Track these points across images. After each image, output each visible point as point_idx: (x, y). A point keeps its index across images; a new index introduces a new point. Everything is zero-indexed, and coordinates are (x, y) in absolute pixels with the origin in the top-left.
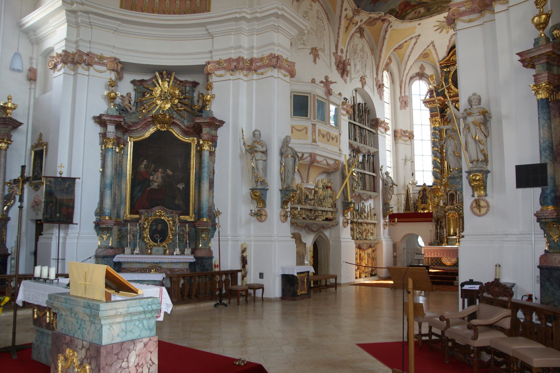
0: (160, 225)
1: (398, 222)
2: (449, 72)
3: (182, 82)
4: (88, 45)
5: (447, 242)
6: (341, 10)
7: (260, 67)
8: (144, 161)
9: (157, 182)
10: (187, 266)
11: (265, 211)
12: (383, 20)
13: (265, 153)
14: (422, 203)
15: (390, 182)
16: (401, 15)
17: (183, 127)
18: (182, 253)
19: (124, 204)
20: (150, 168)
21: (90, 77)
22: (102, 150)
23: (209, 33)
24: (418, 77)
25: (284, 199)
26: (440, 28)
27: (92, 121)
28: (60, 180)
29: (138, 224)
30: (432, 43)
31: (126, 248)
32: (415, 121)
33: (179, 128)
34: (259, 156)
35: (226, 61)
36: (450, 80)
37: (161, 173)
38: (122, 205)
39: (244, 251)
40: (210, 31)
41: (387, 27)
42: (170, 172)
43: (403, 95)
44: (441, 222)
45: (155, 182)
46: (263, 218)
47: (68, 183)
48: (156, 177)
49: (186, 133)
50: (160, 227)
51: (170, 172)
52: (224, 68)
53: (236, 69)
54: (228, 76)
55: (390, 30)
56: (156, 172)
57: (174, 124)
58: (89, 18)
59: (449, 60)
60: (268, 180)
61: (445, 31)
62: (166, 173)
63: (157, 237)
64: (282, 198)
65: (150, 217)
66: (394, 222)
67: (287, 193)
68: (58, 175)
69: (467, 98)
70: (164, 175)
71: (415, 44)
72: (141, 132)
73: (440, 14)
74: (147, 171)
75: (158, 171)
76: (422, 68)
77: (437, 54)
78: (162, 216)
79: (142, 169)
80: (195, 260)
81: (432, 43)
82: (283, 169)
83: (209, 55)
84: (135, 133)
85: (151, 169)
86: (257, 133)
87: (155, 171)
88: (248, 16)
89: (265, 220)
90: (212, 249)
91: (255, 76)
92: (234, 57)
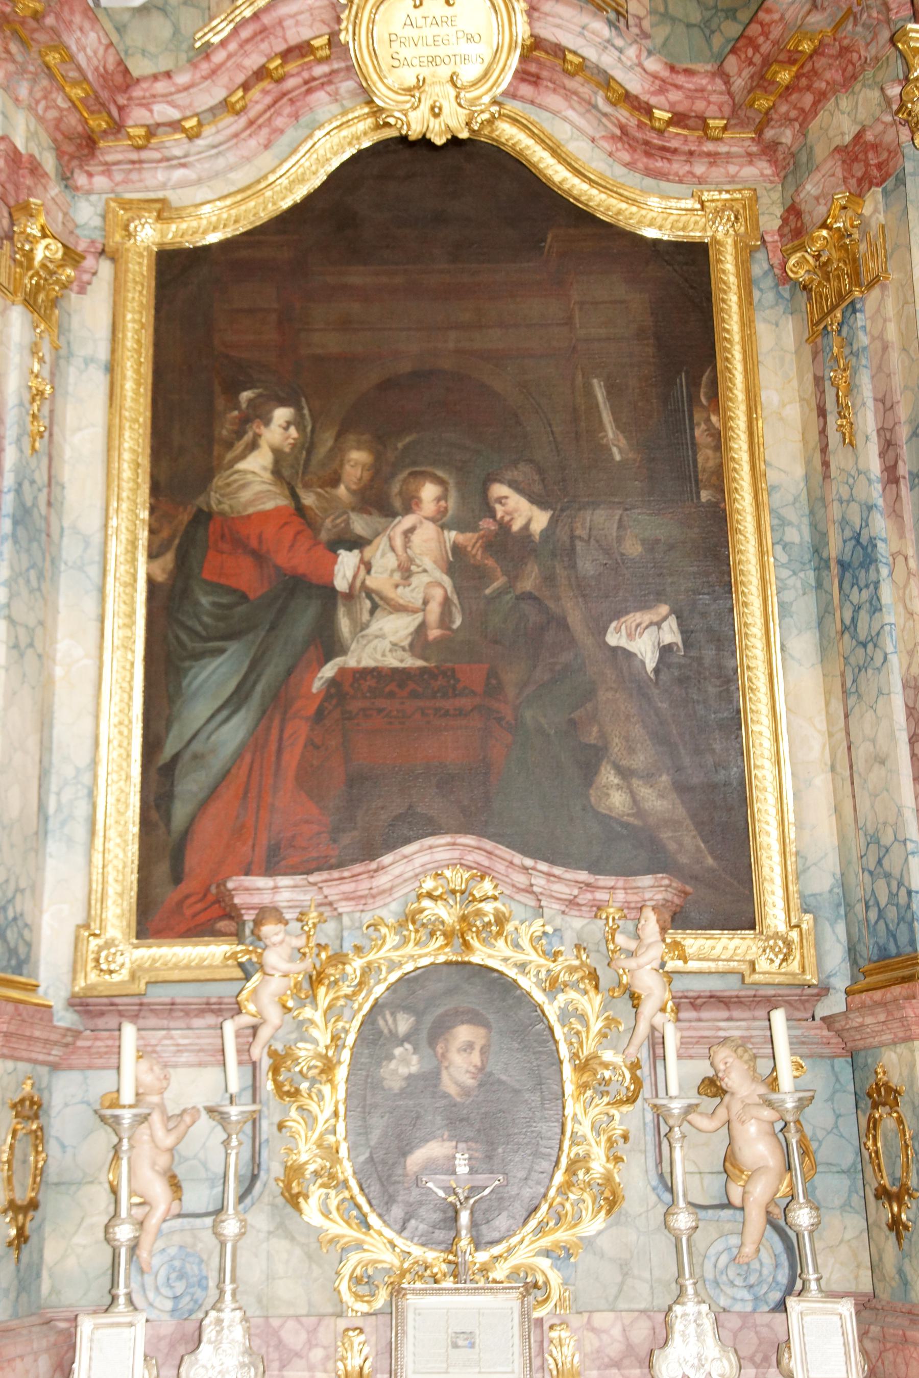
0: (464, 1033)
8: (267, 422)
9: (399, 608)
19: (80, 832)
20: (335, 481)
29: (230, 1027)
31: (86, 1325)
37: (441, 521)
38: (53, 846)
48: (391, 561)
56: (389, 512)
62: (487, 525)
65: (358, 949)
70: (465, 538)
72: (232, 157)
74: (300, 510)
75: (410, 504)
79: (246, 495)
84: (179, 174)
85: (342, 490)
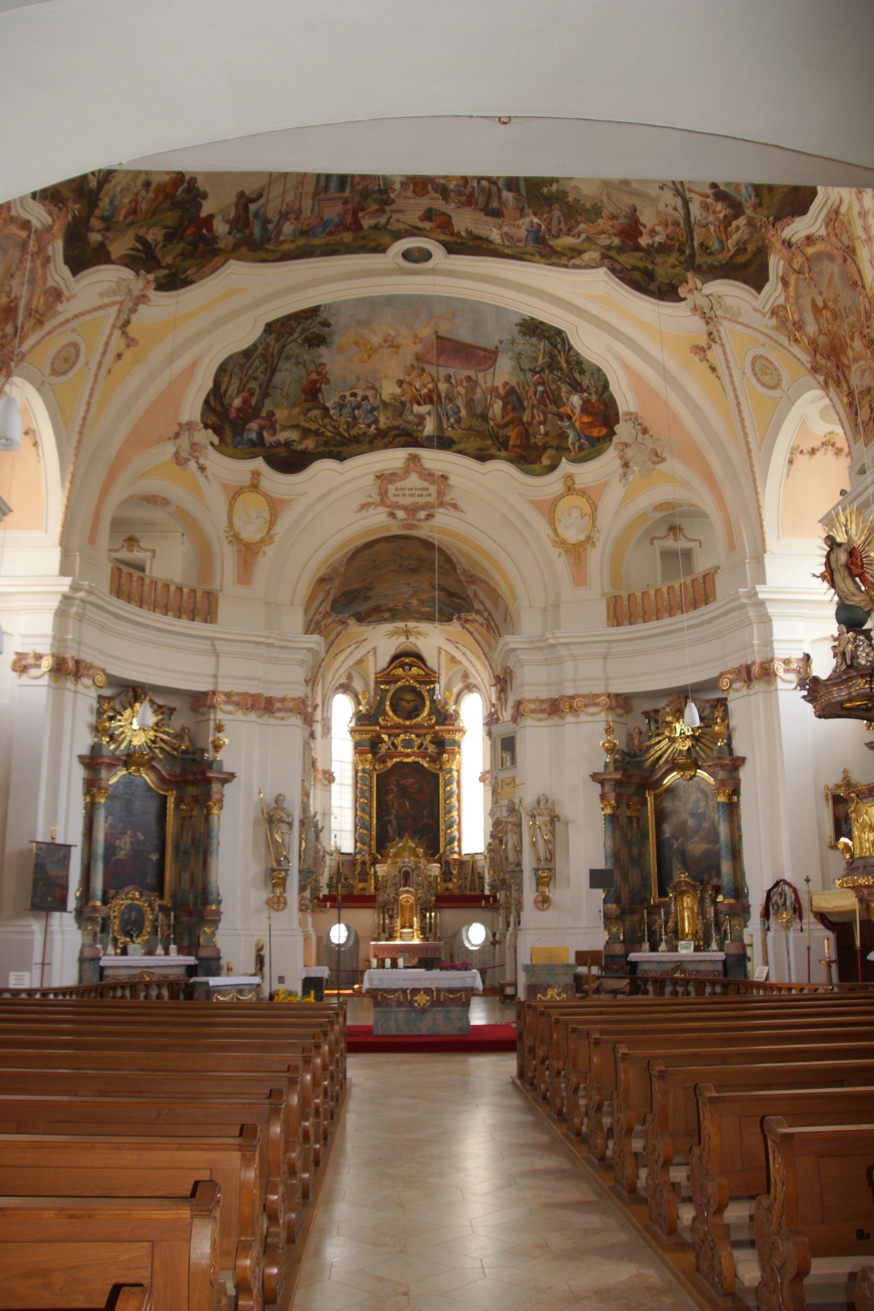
0: (133, 913)
1: (331, 907)
2: (387, 691)
3: (160, 707)
4: (76, 646)
5: (401, 937)
6: (315, 614)
7: (280, 710)
10: (182, 971)
11: (285, 899)
12: (343, 623)
13: (290, 824)
14: (361, 881)
15: (322, 850)
16: (361, 618)
17: (164, 773)
18: (167, 953)
21: (79, 695)
22: (86, 804)
23: (215, 650)
24: (341, 690)
25: (303, 883)
26: (393, 634)
27: (76, 762)
28: (52, 847)
30: (375, 649)
32: (335, 755)
33: (156, 773)
34: (284, 828)
35: (239, 694)
36: (388, 703)
39: (260, 949)
40: (218, 648)
41: (341, 631)
42: (141, 837)
43: (325, 716)
44: (388, 910)
45: (122, 849)
46: (282, 906)
47: (62, 852)
49: (162, 780)
50: (133, 915)
51: (141, 837)
52: (237, 704)
53: (252, 708)
54: (239, 715)
55: (344, 632)
57: (153, 768)
58: (84, 608)
59: (388, 674)
60: (290, 857)
61: (395, 637)
63: (131, 929)
64: (300, 881)
66: (325, 907)
67: (309, 875)
68: (49, 840)
69: (536, 798)
71: (356, 648)
73: (404, 621)
75: (126, 834)
76: (350, 677)
77: (376, 664)
78: (137, 899)
80: (196, 962)
81: (375, 649)
82: (304, 845)
83: (212, 680)
86: (281, 798)
87: (123, 833)
88: (276, 643)
89: (284, 908)
90: (219, 946)
91: (272, 721)
92: (253, 690)
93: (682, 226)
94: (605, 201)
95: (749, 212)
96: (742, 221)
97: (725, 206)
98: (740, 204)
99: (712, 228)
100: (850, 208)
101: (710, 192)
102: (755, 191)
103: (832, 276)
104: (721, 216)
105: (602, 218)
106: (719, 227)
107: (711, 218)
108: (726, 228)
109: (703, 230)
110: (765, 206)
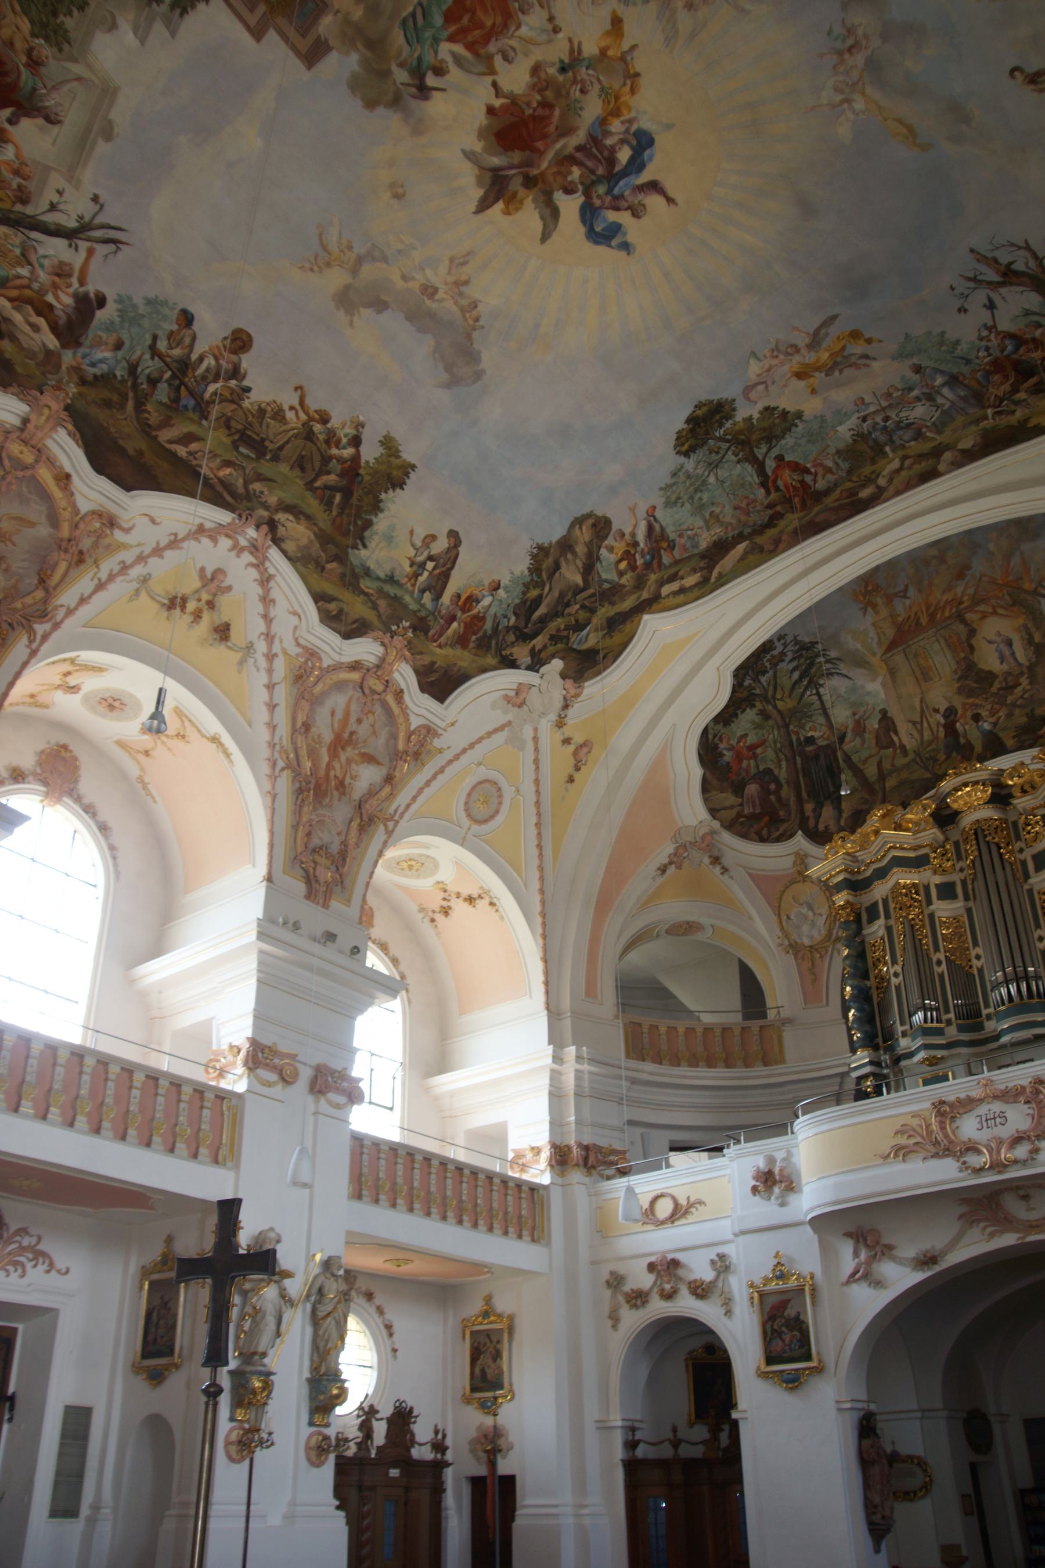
93: (19, 207)
94: (76, 69)
95: (68, 358)
96: (52, 342)
97: (69, 310)
98: (78, 344)
99: (24, 272)
100: (124, 546)
101: (91, 288)
102: (102, 376)
103: (32, 525)
104: (50, 298)
105: (34, 35)
106: (29, 287)
107: (43, 276)
108: (29, 301)
109: (18, 251)
110: (84, 389)
